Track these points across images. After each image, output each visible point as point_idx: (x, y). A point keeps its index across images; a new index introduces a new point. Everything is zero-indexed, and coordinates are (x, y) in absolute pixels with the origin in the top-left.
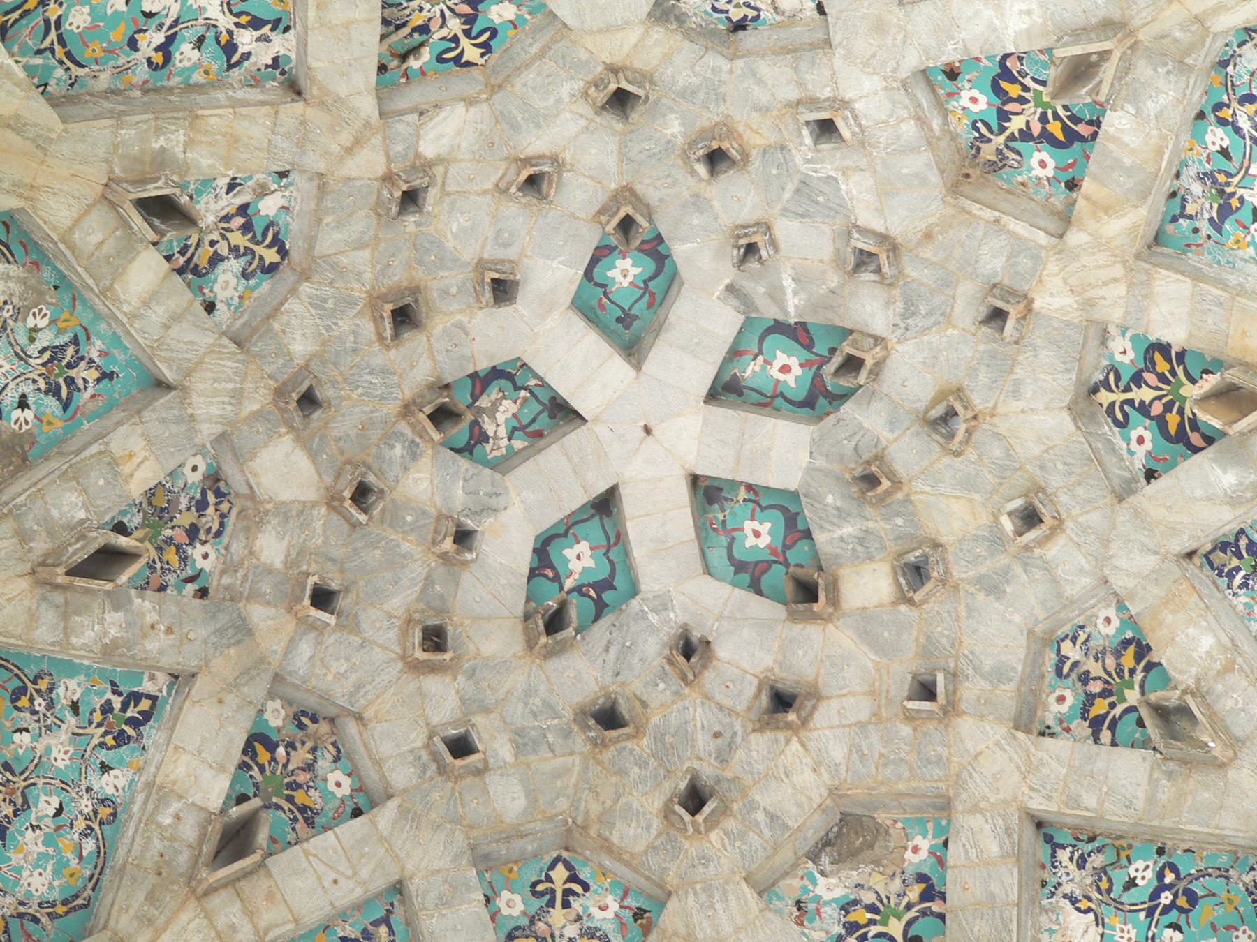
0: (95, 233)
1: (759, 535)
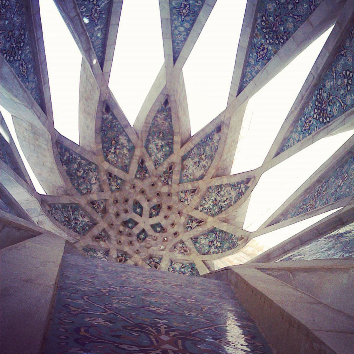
0: (196, 184)
1: (130, 225)
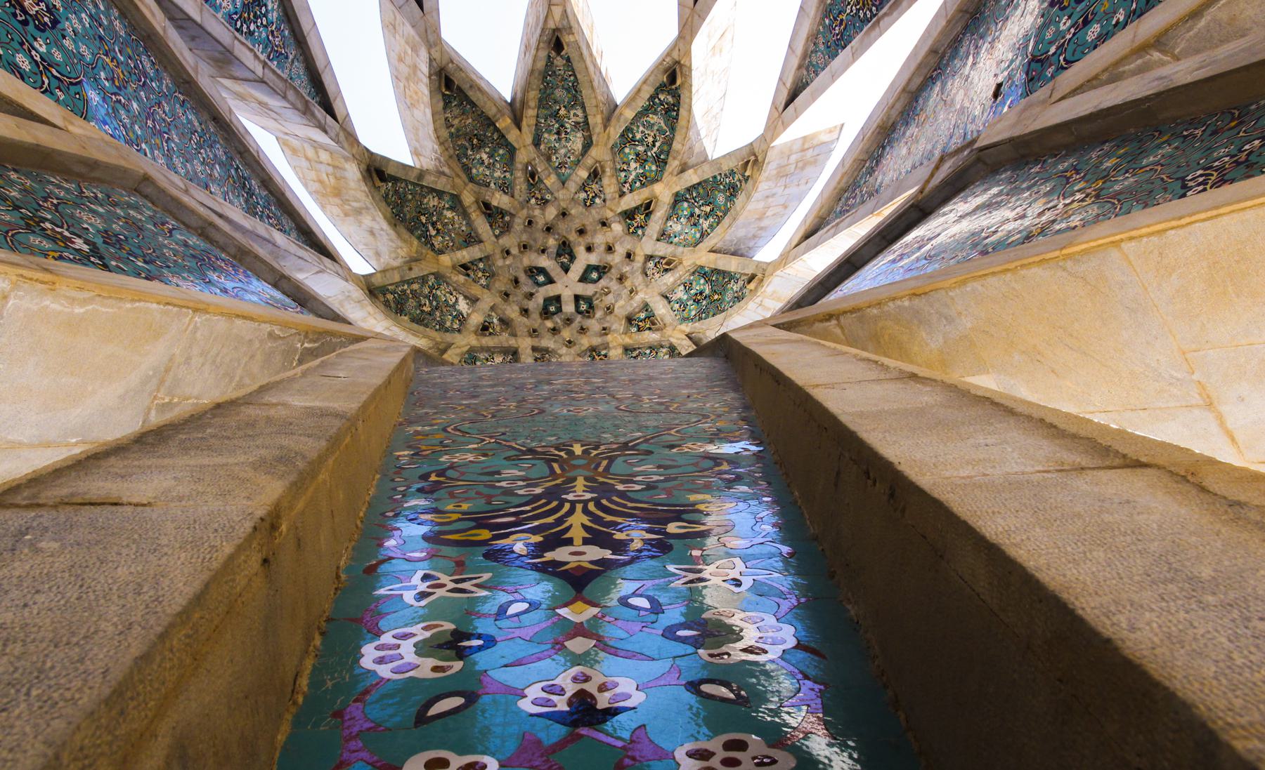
1: (552, 309)
